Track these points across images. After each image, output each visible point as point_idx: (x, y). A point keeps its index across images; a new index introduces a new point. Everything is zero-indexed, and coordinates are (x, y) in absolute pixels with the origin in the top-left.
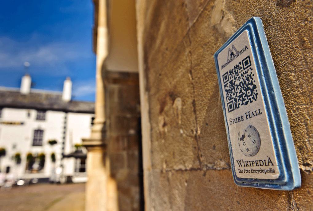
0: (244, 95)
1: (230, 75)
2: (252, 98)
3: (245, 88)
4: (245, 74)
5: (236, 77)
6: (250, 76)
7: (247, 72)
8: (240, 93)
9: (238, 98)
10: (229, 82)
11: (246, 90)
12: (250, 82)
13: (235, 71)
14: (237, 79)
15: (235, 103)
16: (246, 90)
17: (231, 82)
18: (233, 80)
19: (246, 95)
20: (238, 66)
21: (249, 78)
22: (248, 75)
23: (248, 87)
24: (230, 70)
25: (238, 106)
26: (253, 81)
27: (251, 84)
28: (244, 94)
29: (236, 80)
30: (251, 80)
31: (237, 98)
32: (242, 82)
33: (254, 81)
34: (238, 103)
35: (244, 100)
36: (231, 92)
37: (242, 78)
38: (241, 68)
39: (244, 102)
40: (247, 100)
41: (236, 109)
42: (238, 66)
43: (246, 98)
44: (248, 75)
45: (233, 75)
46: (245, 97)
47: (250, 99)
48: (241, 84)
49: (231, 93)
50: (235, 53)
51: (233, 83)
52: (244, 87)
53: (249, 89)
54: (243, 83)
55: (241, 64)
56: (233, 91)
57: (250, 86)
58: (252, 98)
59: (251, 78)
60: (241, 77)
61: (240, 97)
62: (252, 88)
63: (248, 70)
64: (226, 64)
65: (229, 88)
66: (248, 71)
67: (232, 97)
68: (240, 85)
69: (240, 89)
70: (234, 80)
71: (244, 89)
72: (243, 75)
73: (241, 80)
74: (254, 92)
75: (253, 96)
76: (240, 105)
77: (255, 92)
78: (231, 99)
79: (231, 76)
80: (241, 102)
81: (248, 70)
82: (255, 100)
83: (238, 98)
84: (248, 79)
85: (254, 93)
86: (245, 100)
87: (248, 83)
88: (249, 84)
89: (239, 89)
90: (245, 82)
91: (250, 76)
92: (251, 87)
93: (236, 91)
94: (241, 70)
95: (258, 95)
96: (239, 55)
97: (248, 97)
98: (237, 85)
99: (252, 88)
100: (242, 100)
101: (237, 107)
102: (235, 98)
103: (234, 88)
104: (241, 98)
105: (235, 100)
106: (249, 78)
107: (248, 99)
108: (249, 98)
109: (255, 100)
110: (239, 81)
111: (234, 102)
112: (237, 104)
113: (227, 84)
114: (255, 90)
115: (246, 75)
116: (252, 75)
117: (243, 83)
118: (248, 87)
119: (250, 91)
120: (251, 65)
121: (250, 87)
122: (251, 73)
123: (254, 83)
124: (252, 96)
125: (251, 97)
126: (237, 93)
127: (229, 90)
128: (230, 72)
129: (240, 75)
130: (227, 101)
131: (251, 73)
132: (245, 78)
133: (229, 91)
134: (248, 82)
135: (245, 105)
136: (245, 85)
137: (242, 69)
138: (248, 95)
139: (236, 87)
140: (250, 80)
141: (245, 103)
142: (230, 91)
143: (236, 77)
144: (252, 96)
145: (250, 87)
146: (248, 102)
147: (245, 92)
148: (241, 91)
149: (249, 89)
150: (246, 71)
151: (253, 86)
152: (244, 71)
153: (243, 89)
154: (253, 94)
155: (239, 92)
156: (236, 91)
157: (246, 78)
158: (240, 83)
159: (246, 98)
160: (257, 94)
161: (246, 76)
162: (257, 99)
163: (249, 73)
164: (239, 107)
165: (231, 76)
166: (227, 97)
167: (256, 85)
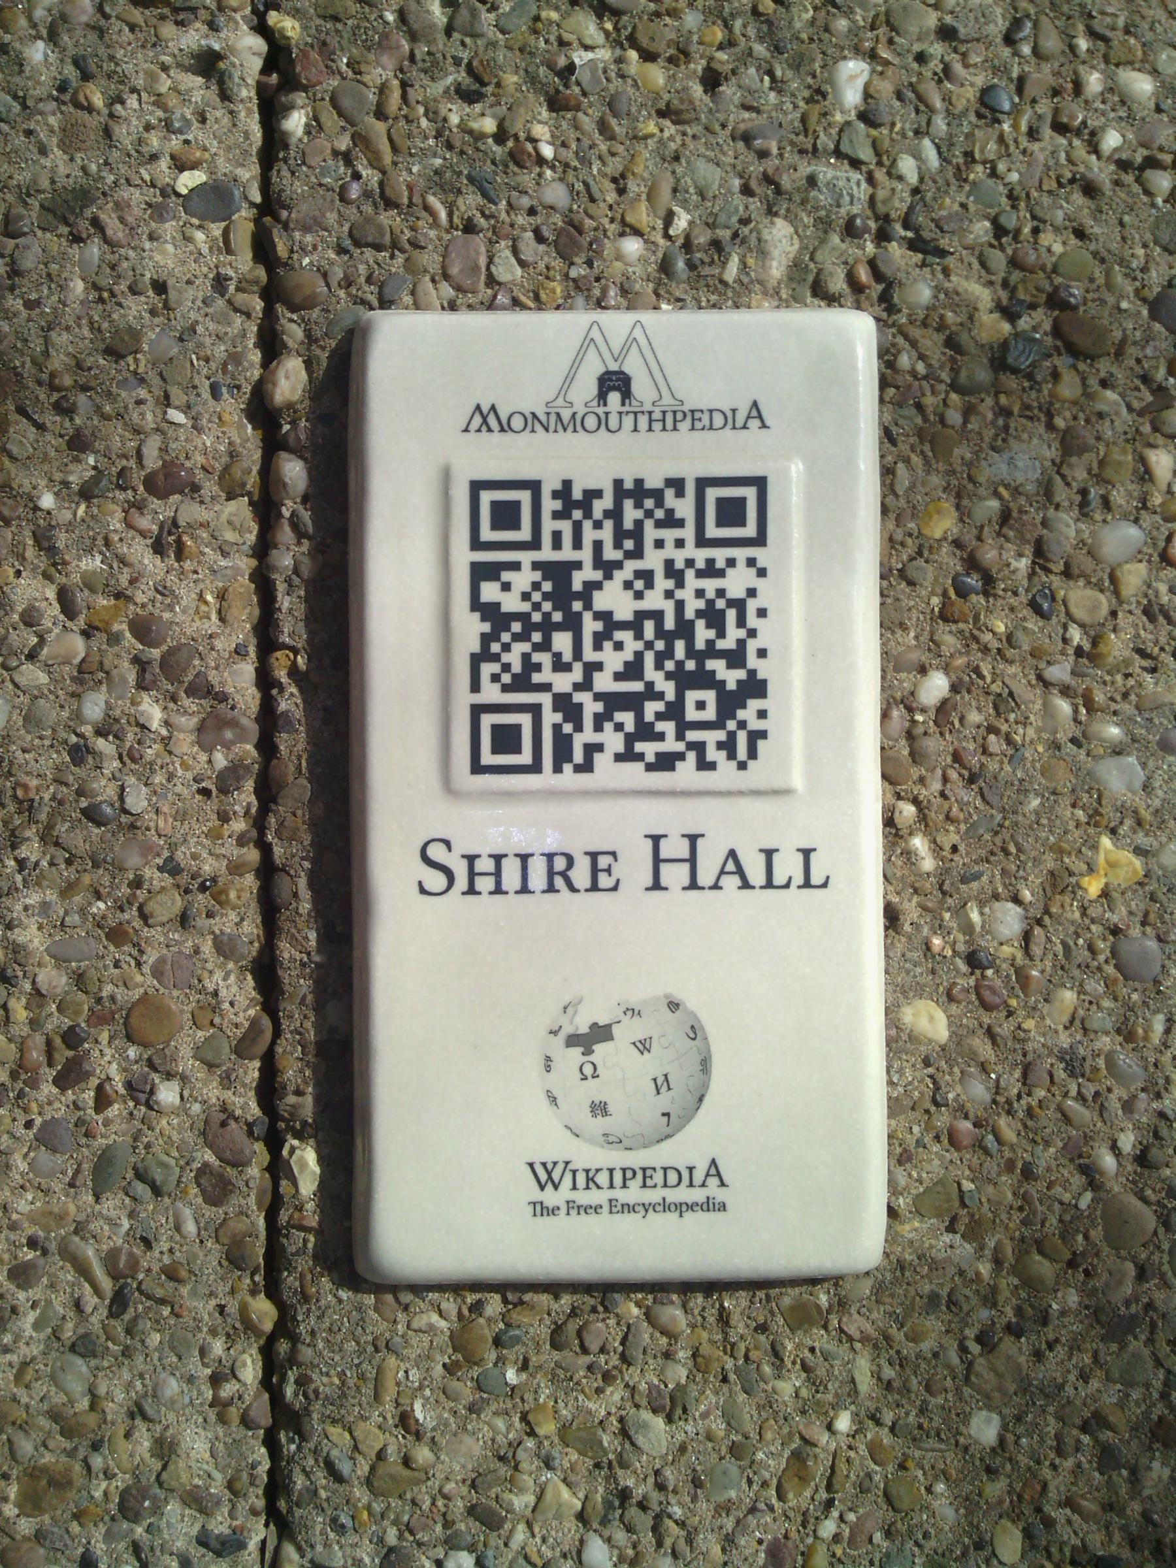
0: (659, 706)
1: (556, 515)
2: (720, 746)
3: (680, 664)
4: (700, 574)
5: (610, 554)
6: (739, 605)
7: (721, 574)
8: (618, 677)
9: (599, 707)
10: (536, 566)
11: (684, 680)
12: (727, 643)
13: (615, 514)
14: (620, 576)
15: (557, 728)
16: (684, 680)
17: (558, 573)
18: (578, 565)
19: (674, 711)
20: (658, 495)
21: (723, 612)
22: (721, 593)
23: (700, 665)
24: (567, 484)
25: (578, 756)
26: (752, 646)
27: (736, 658)
28: (651, 693)
29: (608, 576)
30: (742, 634)
31: (591, 707)
32: (658, 616)
33: (762, 653)
34: (588, 735)
35: (645, 732)
36: (537, 637)
37: (669, 594)
38: (671, 521)
39: (649, 749)
40: (671, 745)
41: (558, 769)
42: (658, 495)
43: (668, 727)
44: (721, 593)
45: (589, 534)
46: (659, 716)
47: (699, 748)
48: (649, 628)
49: (537, 647)
50: (641, 388)
51: (577, 586)
52: (669, 653)
53: (706, 680)
54: (669, 624)
55: (680, 494)
56: (562, 642)
57: (717, 666)
58: (720, 746)
59: (741, 622)
60: (662, 583)
61: (613, 702)
62: (731, 686)
63: (731, 563)
64: (532, 421)
65: (526, 607)
66: (730, 572)
67: (536, 678)
68: (635, 625)
69: (628, 655)
70: (588, 573)
71: (670, 665)
72: (682, 572)
73: (654, 600)
74: (741, 714)
75: (732, 736)
76: (602, 761)
77: (748, 713)
78: (522, 683)
79: (566, 527)
80: (614, 742)
81: (731, 563)
82: (734, 764)
83: (599, 707)
84: (715, 619)
85: (742, 725)
86: (661, 737)
87: (710, 643)
88: (711, 651)
89: (619, 646)
90: (685, 629)
91: (739, 605)
92: (732, 678)
93: (589, 655)
94: (669, 535)
95: (761, 744)
96: (684, 426)
97: (683, 727)
98: (605, 616)
99: (731, 686)
100: (630, 727)
101: (570, 759)
102: (570, 695)
103: (573, 624)
104: (627, 719)
105: (566, 706)
106: (723, 612)
107: (680, 737)
108: (692, 736)
109: (734, 764)
110: (639, 595)
111: (550, 718)
112: (579, 741)
113: (515, 566)
114: (754, 705)
115: (710, 586)
116: (752, 606)
117: (669, 624)
118: (700, 665)
119: (709, 696)
120: (760, 540)
121: (719, 677)
122: (752, 593)
123: (752, 661)
124: (721, 735)
125: (712, 737)
126: (599, 666)
127: (523, 617)
128: (564, 491)
129: (653, 560)
130: (475, 687)
131: (752, 593)
132: (693, 606)
133: (516, 627)
134: (711, 634)
135: (650, 768)
136: (680, 647)
137: (688, 533)
138: (692, 714)
139: (590, 626)
141: (650, 758)
142: (529, 626)
143: (610, 554)
144: (721, 735)
145: (719, 677)
146: (681, 756)
147: (669, 689)
148: (633, 670)
149: (706, 680)
150: (710, 562)
151: (741, 674)
152: (701, 556)
153: (659, 666)
154: (731, 725)
155: (620, 668)
156: (589, 655)
157: (701, 604)
158: (641, 616)
160: (763, 734)
162: (751, 763)
163: (736, 583)
164: (586, 767)
165: (566, 527)
166: (476, 660)
167: (764, 682)
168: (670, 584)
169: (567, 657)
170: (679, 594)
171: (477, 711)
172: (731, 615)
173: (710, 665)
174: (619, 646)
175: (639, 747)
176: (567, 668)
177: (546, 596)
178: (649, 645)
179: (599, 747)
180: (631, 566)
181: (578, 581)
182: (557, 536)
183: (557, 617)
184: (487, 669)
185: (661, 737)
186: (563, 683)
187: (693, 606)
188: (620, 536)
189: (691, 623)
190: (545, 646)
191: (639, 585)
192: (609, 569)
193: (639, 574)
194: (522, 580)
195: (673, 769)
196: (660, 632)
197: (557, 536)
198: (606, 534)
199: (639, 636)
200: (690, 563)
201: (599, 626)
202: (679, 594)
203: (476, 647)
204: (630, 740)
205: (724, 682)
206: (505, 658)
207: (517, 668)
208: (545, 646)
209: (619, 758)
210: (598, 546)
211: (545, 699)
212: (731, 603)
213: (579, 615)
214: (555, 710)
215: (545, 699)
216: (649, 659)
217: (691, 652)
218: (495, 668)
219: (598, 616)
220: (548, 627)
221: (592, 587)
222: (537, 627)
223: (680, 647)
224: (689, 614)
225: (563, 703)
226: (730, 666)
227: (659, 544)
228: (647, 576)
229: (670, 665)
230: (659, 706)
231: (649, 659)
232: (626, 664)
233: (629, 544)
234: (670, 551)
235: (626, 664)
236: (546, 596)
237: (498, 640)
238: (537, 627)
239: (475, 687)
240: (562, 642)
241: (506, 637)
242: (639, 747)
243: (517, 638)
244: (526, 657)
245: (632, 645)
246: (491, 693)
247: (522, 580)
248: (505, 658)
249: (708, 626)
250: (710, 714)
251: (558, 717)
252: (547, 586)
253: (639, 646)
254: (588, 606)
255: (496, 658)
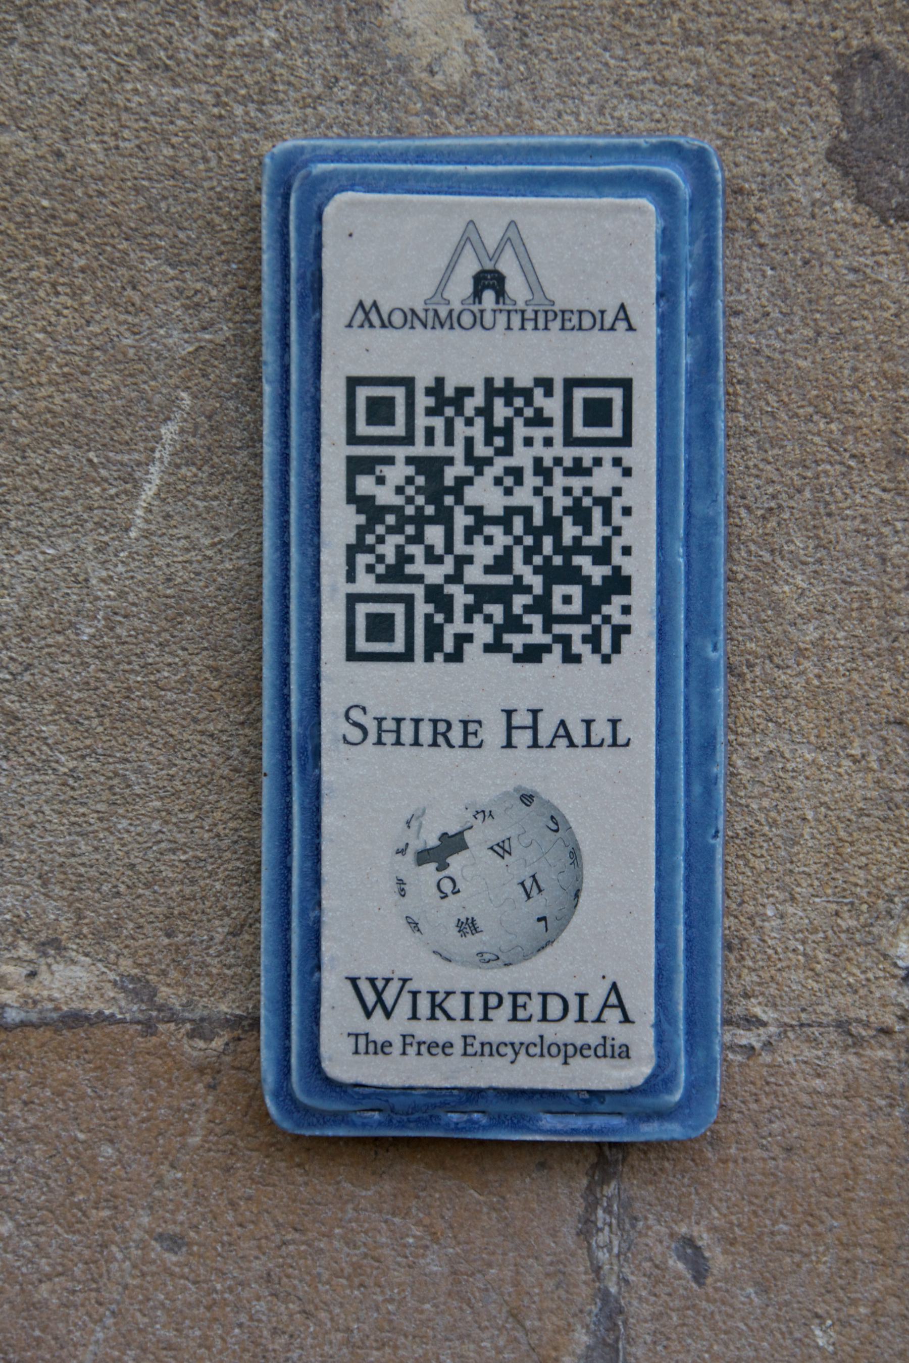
2: (585, 639)
5: (481, 450)
8: (488, 570)
13: (486, 411)
14: (490, 472)
15: (428, 618)
17: (431, 467)
21: (589, 510)
22: (587, 491)
26: (617, 543)
28: (520, 587)
32: (527, 512)
34: (458, 626)
37: (537, 491)
39: (517, 641)
43: (535, 620)
48: (518, 523)
49: (410, 540)
52: (537, 548)
54: (538, 520)
59: (607, 520)
60: (531, 480)
70: (460, 469)
73: (523, 496)
74: (606, 610)
78: (395, 574)
80: (483, 632)
94: (539, 433)
102: (440, 587)
104: (496, 611)
107: (547, 629)
111: (422, 608)
114: (618, 600)
115: (577, 483)
125: (577, 631)
127: (397, 510)
129: (522, 457)
130: (351, 577)
135: (517, 659)
136: (548, 542)
139: (462, 521)
140: (599, 531)
148: (502, 564)
149: (572, 575)
155: (491, 562)
156: (460, 547)
157: (569, 502)
159: (535, 620)
161: (567, 491)
166: (352, 551)
168: (539, 481)
169: (439, 550)
170: (547, 491)
171: (353, 600)
172: (597, 514)
173: (577, 560)
174: (489, 541)
175: (507, 638)
176: (439, 560)
177: (419, 490)
178: (518, 540)
179: (469, 638)
180: (501, 463)
181: (449, 476)
182: (430, 433)
183: (430, 510)
184: (363, 560)
185: (528, 629)
186: (435, 574)
187: (560, 503)
188: (490, 432)
189: (559, 520)
190: (418, 538)
191: (509, 481)
192: (479, 464)
193: (508, 471)
194: (396, 474)
195: (539, 661)
196: (529, 528)
197: (430, 433)
198: (478, 430)
199: (508, 531)
200: (558, 461)
201: (470, 520)
202: (547, 491)
203: (352, 540)
204: (499, 631)
205: (589, 578)
206: (380, 549)
207: (391, 559)
208: (418, 538)
209: (488, 648)
210: (469, 442)
211: (418, 591)
212: (598, 501)
213: (451, 509)
214: (428, 600)
215: (418, 591)
216: (518, 554)
217: (558, 548)
218: (370, 559)
219: (469, 510)
220: (420, 520)
221: (464, 481)
222: (410, 520)
223: (548, 542)
224: (557, 511)
225: (435, 594)
226: (595, 563)
227: (528, 442)
228: (517, 473)
229: (538, 560)
230: (527, 599)
231: (518, 554)
232: (496, 558)
233: (499, 441)
234: (538, 449)
235: (496, 558)
236: (419, 490)
237: (373, 532)
238: (410, 520)
239: (351, 577)
240: (434, 534)
241: (380, 529)
242: (507, 638)
243: (391, 530)
244: (399, 549)
245: (501, 540)
246: (366, 584)
247: (396, 474)
248: (380, 549)
249: (575, 523)
250: (576, 608)
251: (430, 608)
252: (420, 480)
253: (509, 540)
254: (459, 500)
255: (371, 550)
